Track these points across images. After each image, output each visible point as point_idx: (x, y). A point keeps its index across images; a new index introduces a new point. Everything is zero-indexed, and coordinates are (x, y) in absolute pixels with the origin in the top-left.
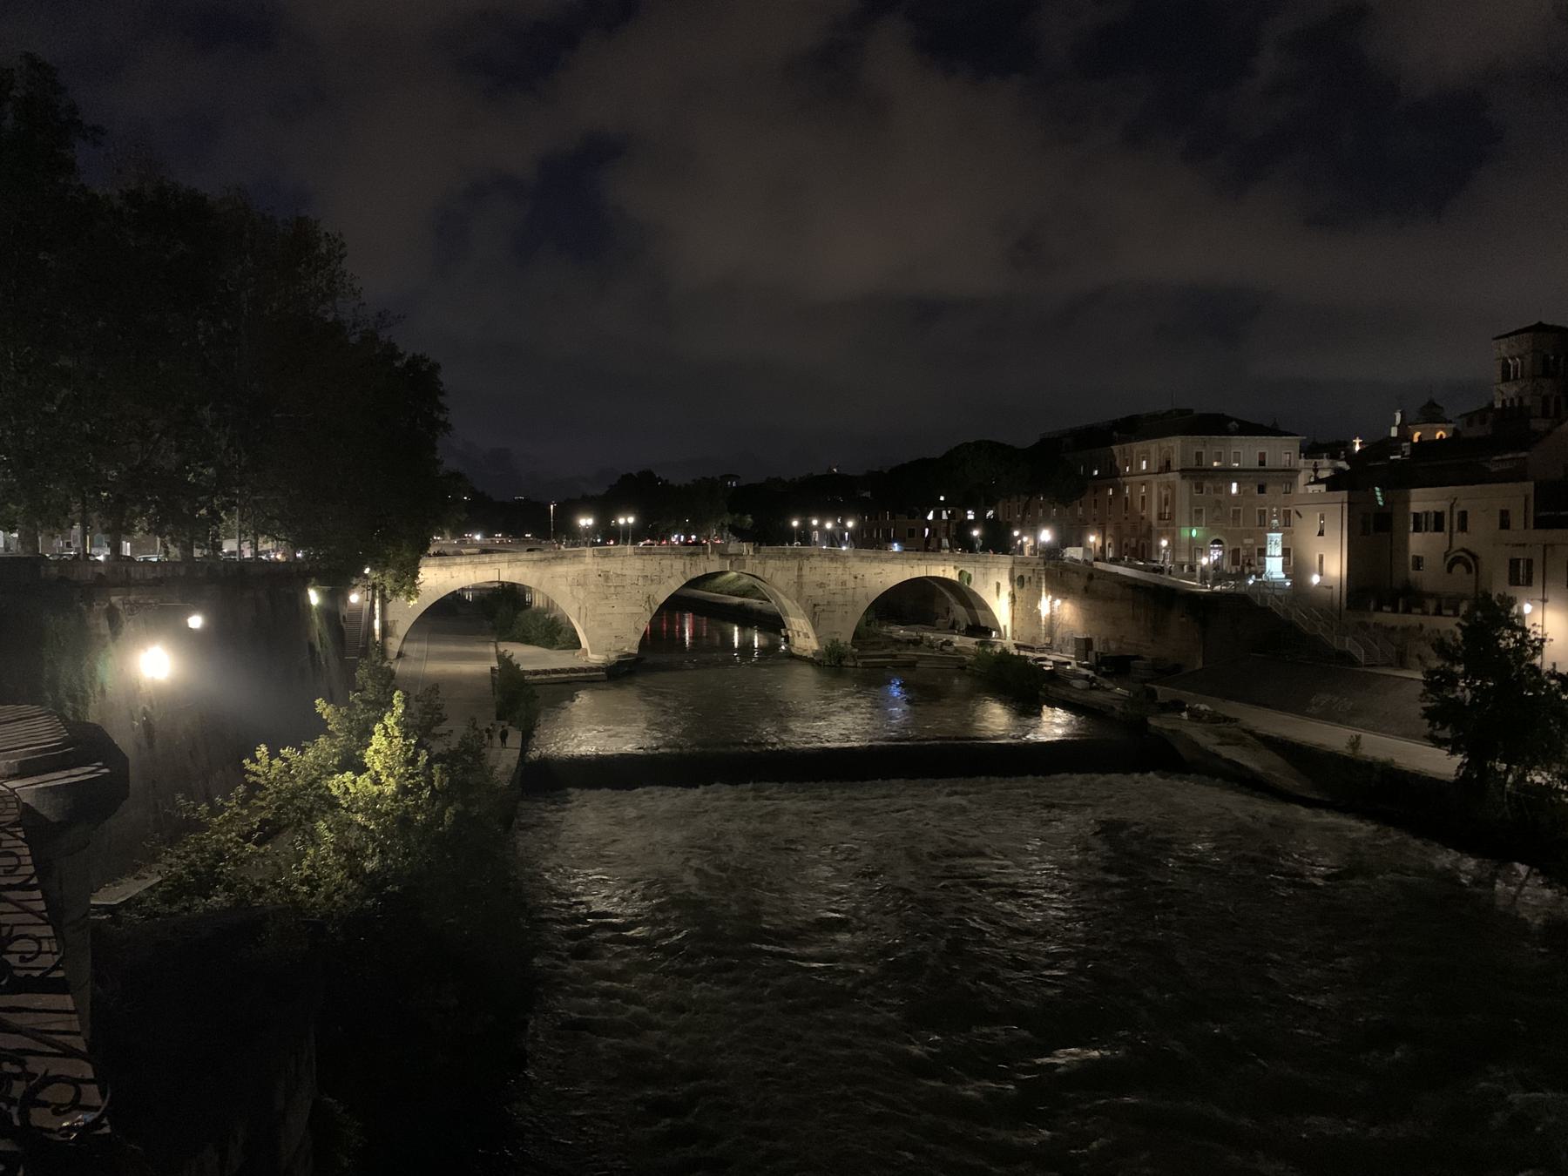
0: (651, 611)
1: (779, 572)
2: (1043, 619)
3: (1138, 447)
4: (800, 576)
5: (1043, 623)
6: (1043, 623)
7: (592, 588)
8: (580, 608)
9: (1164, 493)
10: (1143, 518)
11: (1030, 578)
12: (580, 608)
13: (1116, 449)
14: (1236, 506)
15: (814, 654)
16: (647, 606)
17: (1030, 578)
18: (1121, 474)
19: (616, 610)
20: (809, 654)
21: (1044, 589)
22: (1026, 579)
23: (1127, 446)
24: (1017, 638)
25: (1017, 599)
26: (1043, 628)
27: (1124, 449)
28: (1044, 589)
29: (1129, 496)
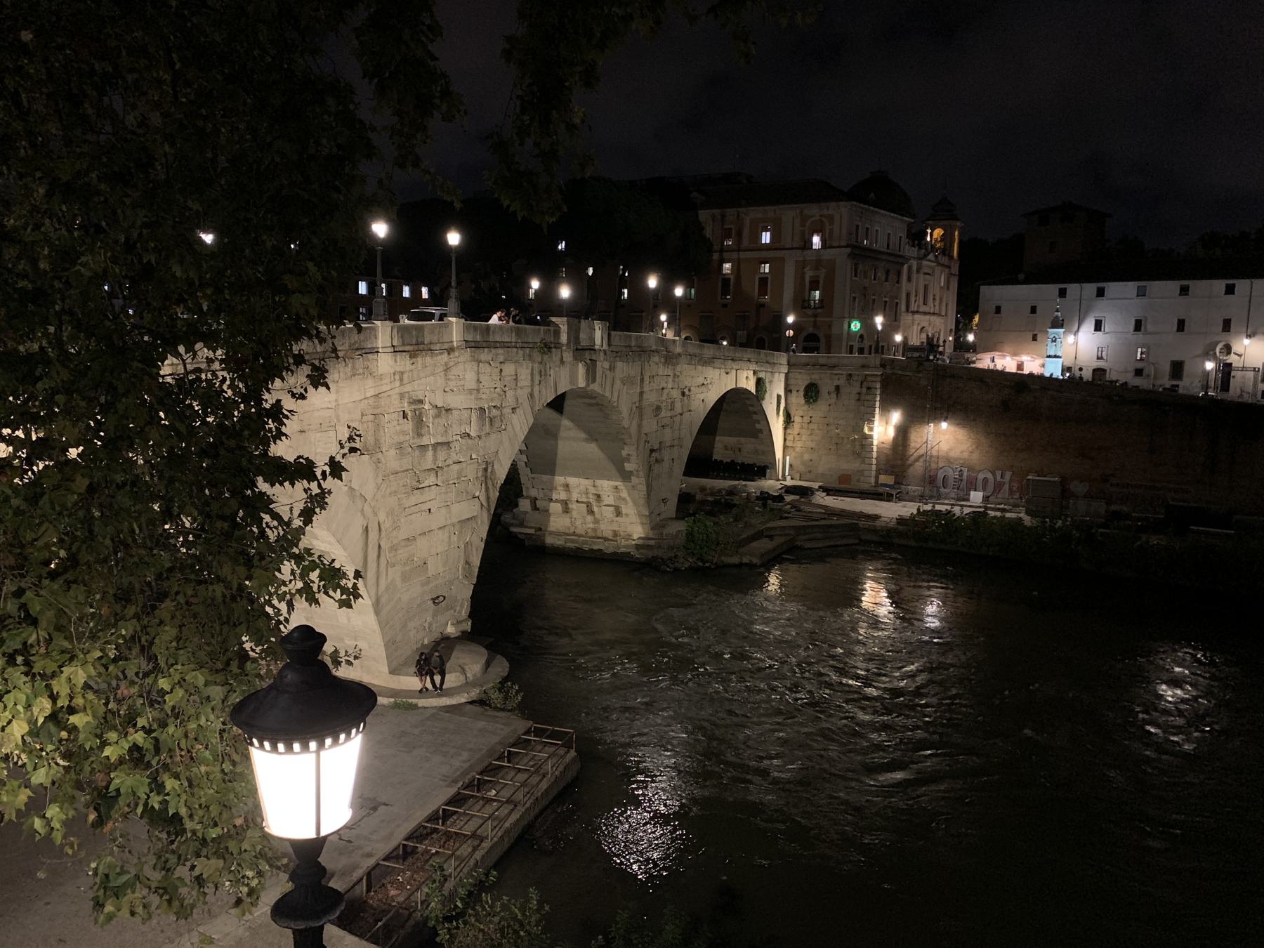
0: (489, 511)
1: (625, 387)
2: (875, 449)
3: (754, 213)
4: (641, 393)
5: (875, 455)
6: (875, 455)
7: (390, 458)
8: (366, 530)
9: (809, 274)
10: (763, 305)
11: (837, 388)
12: (366, 530)
13: (704, 215)
14: (874, 295)
15: (637, 547)
16: (483, 498)
17: (837, 388)
18: (716, 247)
19: (440, 518)
20: (623, 546)
21: (878, 404)
22: (824, 391)
23: (731, 213)
24: (797, 476)
25: (797, 419)
26: (874, 461)
27: (723, 216)
28: (878, 404)
29: (732, 277)
